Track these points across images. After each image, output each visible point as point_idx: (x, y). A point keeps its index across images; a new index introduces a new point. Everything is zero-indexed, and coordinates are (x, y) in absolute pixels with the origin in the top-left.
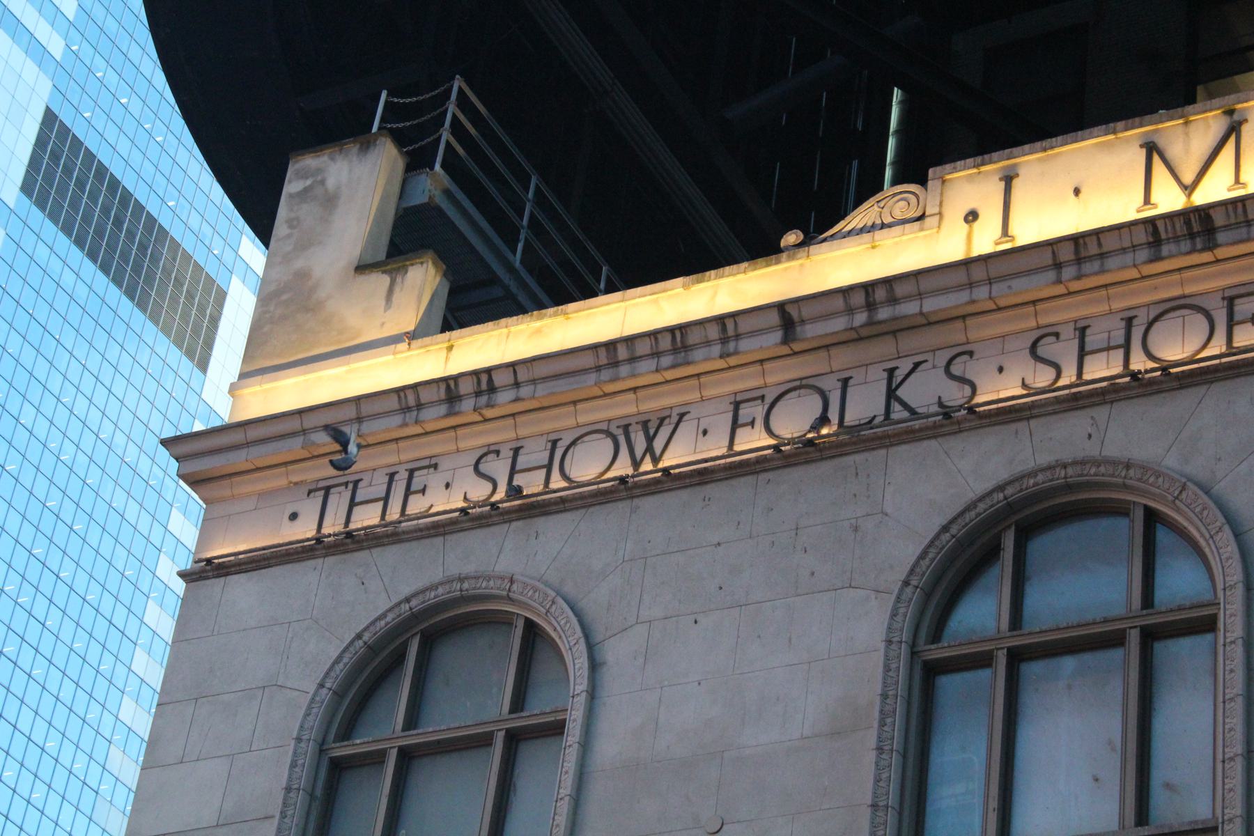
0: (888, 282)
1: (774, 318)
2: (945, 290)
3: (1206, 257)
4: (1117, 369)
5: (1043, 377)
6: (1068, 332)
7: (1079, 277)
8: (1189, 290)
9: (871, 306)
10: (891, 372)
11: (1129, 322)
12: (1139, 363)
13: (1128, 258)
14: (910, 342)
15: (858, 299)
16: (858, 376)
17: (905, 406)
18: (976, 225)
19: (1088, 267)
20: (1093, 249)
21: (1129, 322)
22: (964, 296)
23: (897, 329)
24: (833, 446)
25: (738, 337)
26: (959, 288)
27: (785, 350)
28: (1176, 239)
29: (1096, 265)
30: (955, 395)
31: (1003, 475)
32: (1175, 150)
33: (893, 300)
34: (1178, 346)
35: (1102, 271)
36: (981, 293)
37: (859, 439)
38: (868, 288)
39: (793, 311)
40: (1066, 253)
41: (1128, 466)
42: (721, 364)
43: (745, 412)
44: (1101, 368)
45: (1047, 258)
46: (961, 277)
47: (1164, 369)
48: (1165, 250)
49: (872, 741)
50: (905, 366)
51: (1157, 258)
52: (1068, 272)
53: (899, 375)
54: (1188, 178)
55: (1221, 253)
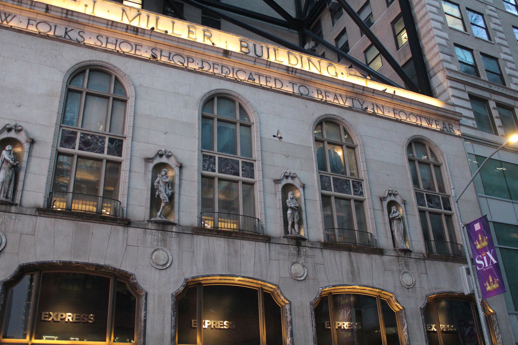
0: (73, 11)
1: (45, 6)
2: (84, 18)
3: (135, 36)
4: (114, 48)
5: (99, 44)
6: (104, 37)
7: (111, 28)
8: (129, 40)
9: (67, 14)
10: (66, 29)
11: (117, 40)
12: (118, 49)
13: (121, 29)
14: (71, 24)
15: (65, 12)
16: (58, 26)
17: (69, 37)
18: (87, 8)
19: (113, 27)
20: (115, 24)
21: (117, 40)
22: (87, 21)
23: (70, 21)
24: (52, 38)
25: (34, 6)
26: (87, 19)
27: (44, 14)
28: (131, 30)
29: (115, 28)
30: (80, 39)
31: (89, 59)
32: (128, 13)
33: (72, 15)
34: (126, 49)
35: (116, 29)
36: (91, 22)
37: (56, 38)
38: (68, 10)
39: (50, 7)
40: (110, 23)
41: (115, 67)
42: (28, 10)
43: (31, 22)
44: (110, 47)
45: (106, 22)
46: (88, 17)
47: (40, 33)
48: (128, 31)
49: (58, 100)
50: (69, 29)
51: (127, 32)
52: (109, 26)
53: (68, 30)
54: (130, 20)
55: (137, 36)
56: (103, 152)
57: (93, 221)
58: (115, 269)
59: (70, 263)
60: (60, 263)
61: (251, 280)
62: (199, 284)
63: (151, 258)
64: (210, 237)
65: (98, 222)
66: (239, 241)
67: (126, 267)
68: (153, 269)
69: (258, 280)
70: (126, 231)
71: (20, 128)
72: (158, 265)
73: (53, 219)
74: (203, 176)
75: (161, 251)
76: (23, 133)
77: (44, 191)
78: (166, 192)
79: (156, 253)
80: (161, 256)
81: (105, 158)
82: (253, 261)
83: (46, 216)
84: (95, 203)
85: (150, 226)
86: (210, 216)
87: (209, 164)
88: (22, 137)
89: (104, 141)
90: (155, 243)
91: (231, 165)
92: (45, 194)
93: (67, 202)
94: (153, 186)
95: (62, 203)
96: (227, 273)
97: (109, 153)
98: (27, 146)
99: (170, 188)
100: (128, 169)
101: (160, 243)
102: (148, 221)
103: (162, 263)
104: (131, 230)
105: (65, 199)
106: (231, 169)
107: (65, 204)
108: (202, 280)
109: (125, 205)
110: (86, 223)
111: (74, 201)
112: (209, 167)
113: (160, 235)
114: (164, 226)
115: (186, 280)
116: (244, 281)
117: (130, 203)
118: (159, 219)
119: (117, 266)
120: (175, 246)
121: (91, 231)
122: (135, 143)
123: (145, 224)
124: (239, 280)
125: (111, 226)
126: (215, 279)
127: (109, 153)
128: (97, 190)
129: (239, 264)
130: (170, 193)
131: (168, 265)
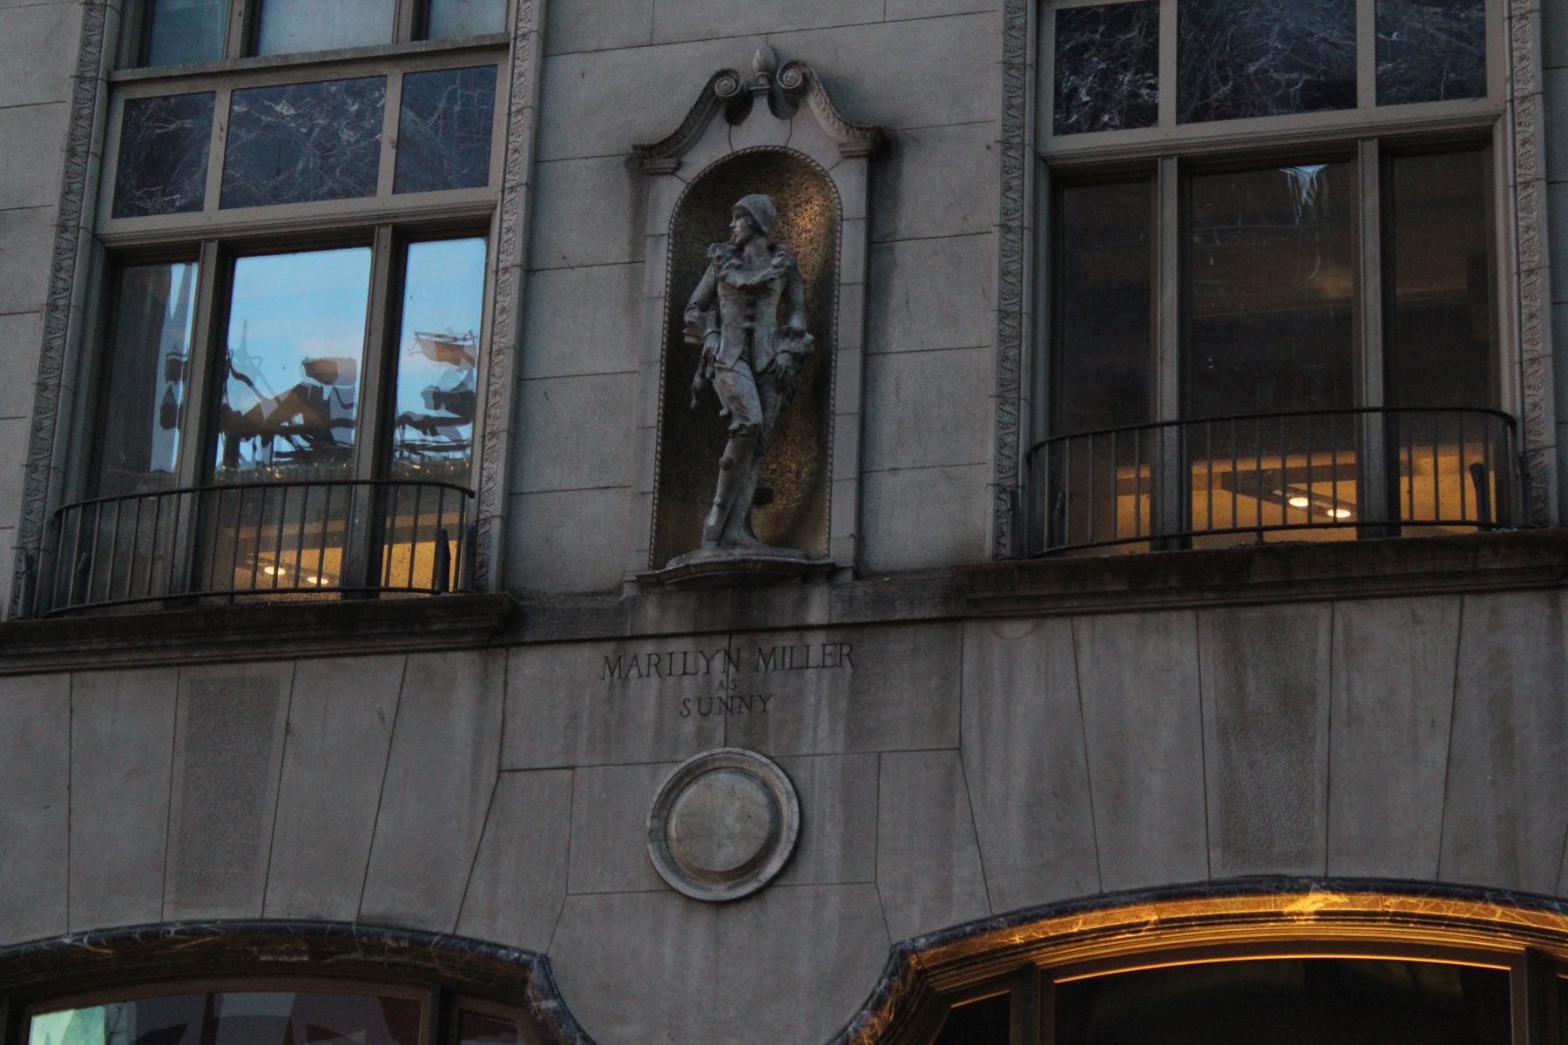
56: (1344, 97)
57: (291, 649)
58: (419, 941)
59: (153, 935)
60: (93, 943)
61: (1420, 906)
62: (1024, 972)
63: (659, 834)
64: (1084, 624)
65: (314, 648)
66: (1321, 612)
67: (499, 921)
68: (673, 910)
69: (1474, 894)
70: (498, 680)
71: (792, 78)
72: (705, 875)
73: (65, 678)
74: (1063, 180)
75: (722, 779)
76: (816, 104)
77: (14, 516)
78: (748, 357)
79: (690, 793)
80: (728, 808)
81: (1366, 133)
82: (1435, 751)
83: (22, 665)
84: (1348, 459)
85: (651, 615)
86: (1331, 448)
87: (1103, 76)
88: (815, 135)
89: (377, 112)
90: (689, 727)
91: (1285, 36)
92: (23, 533)
93: (1358, 473)
94: (675, 324)
95: (310, 557)
96: (1220, 874)
97: (1383, 99)
98: (849, 184)
99: (797, 322)
100: (1539, 169)
101: (718, 722)
102: (644, 583)
103: (729, 855)
104: (530, 666)
105: (1145, 473)
106: (1290, 66)
107: (1145, 501)
108: (1029, 945)
109: (495, 505)
110: (253, 670)
111: (1199, 470)
112: (1103, 97)
113: (718, 663)
114: (739, 602)
115: (900, 956)
116: (1370, 917)
117: (531, 481)
118: (706, 554)
119: (439, 922)
120: (824, 729)
121: (281, 715)
122: (564, 67)
123: (620, 611)
124: (1322, 916)
125: (404, 657)
126: (1132, 928)
127: (1384, 97)
128: (1345, 376)
129: (1319, 793)
130: (782, 360)
131: (774, 866)
